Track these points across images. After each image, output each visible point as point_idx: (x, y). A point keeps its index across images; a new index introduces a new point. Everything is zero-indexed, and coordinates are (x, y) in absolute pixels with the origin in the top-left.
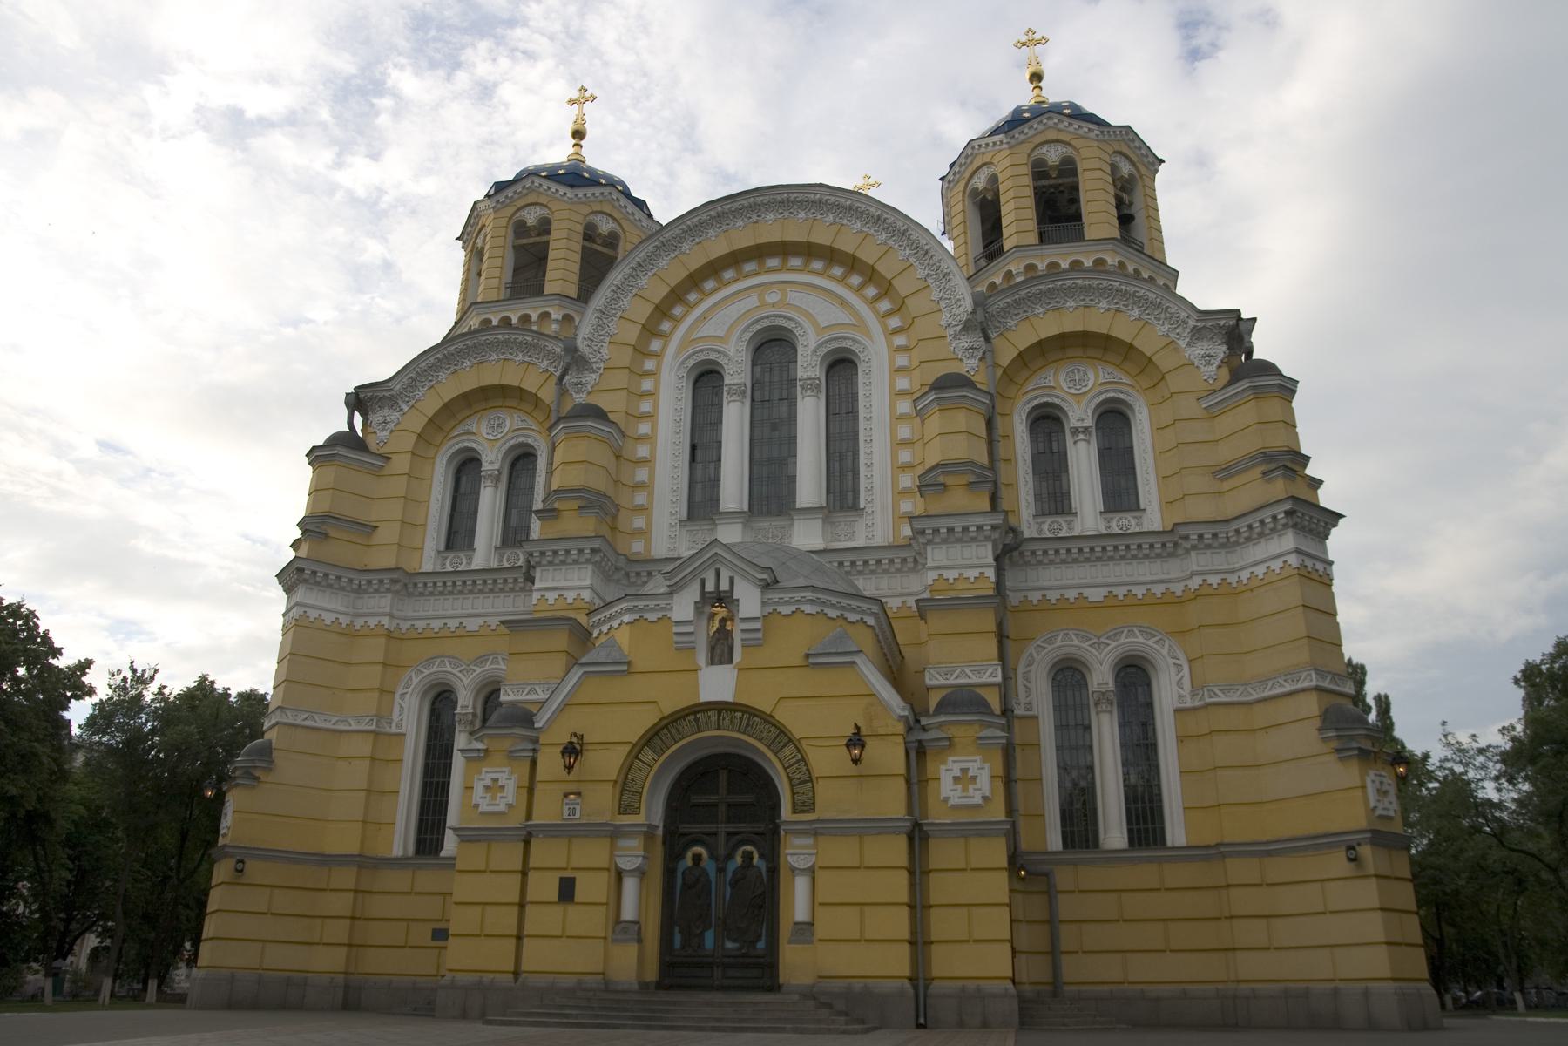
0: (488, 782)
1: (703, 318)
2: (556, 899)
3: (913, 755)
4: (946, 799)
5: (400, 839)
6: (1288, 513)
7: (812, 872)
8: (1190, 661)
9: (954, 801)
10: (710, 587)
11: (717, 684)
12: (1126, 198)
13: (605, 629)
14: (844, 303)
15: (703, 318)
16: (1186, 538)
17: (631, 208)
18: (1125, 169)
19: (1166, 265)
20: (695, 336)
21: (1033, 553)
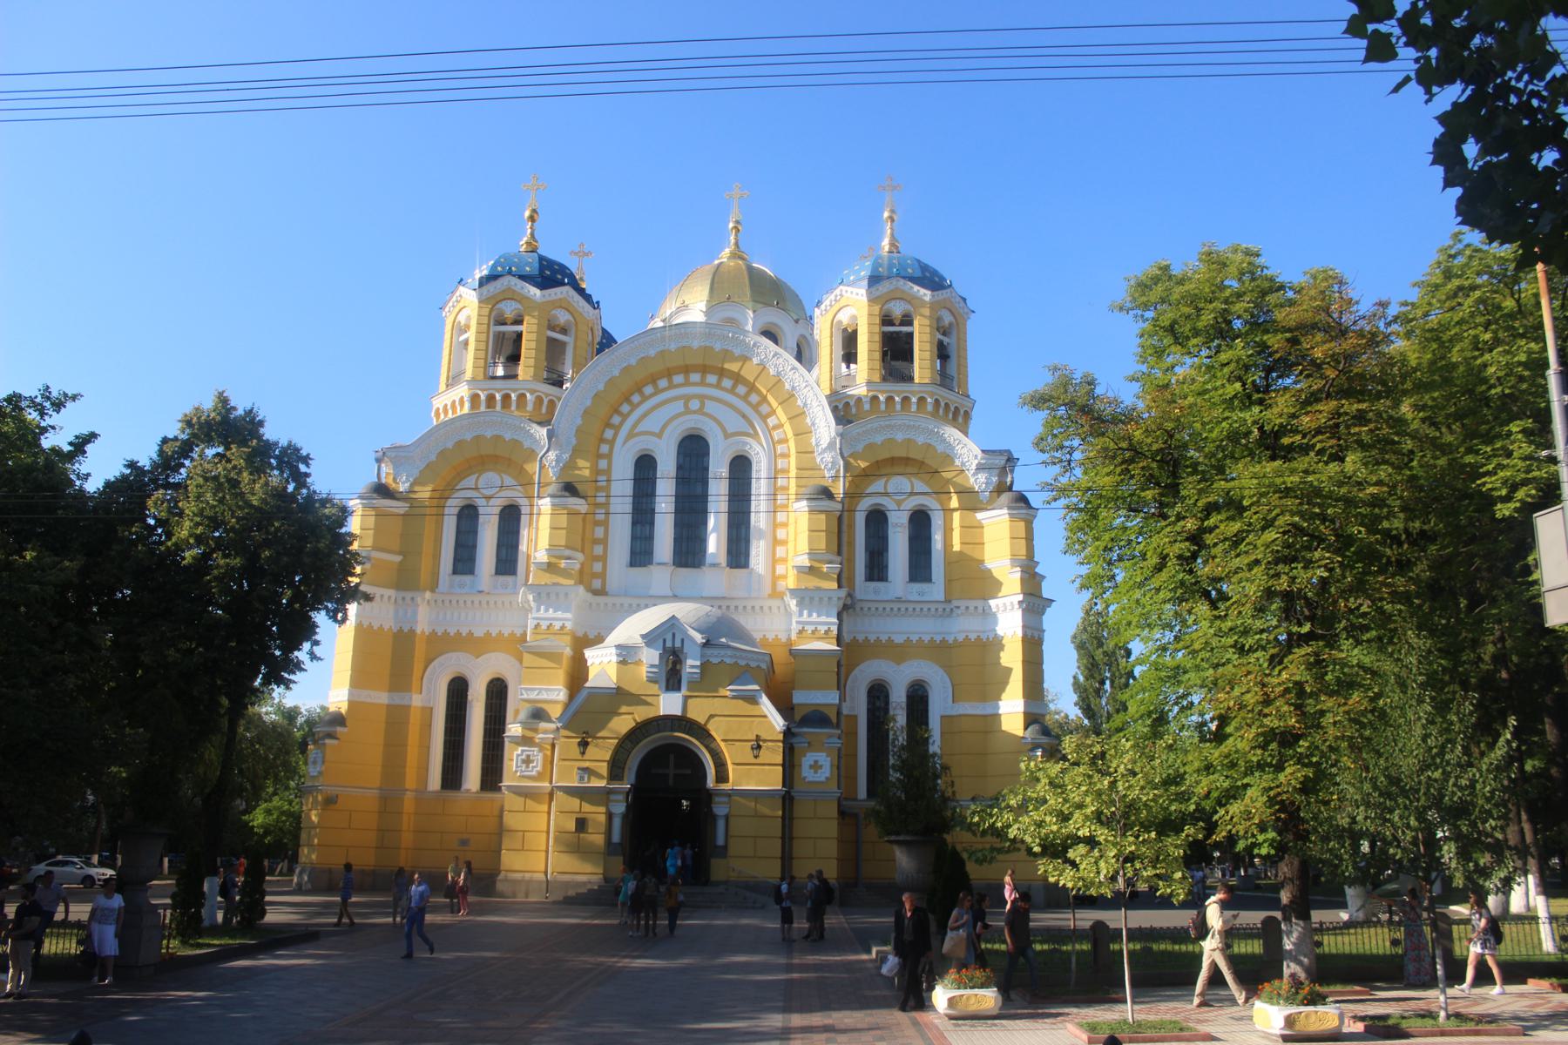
0: (524, 757)
1: (644, 416)
2: (574, 830)
3: (787, 751)
4: (805, 778)
5: (435, 780)
6: (1020, 602)
7: (727, 818)
8: (953, 686)
9: (811, 779)
10: (669, 644)
11: (669, 704)
12: (946, 340)
13: (597, 661)
14: (744, 416)
15: (644, 416)
16: (958, 607)
17: (582, 302)
18: (947, 319)
19: (968, 396)
20: (636, 431)
21: (862, 609)
